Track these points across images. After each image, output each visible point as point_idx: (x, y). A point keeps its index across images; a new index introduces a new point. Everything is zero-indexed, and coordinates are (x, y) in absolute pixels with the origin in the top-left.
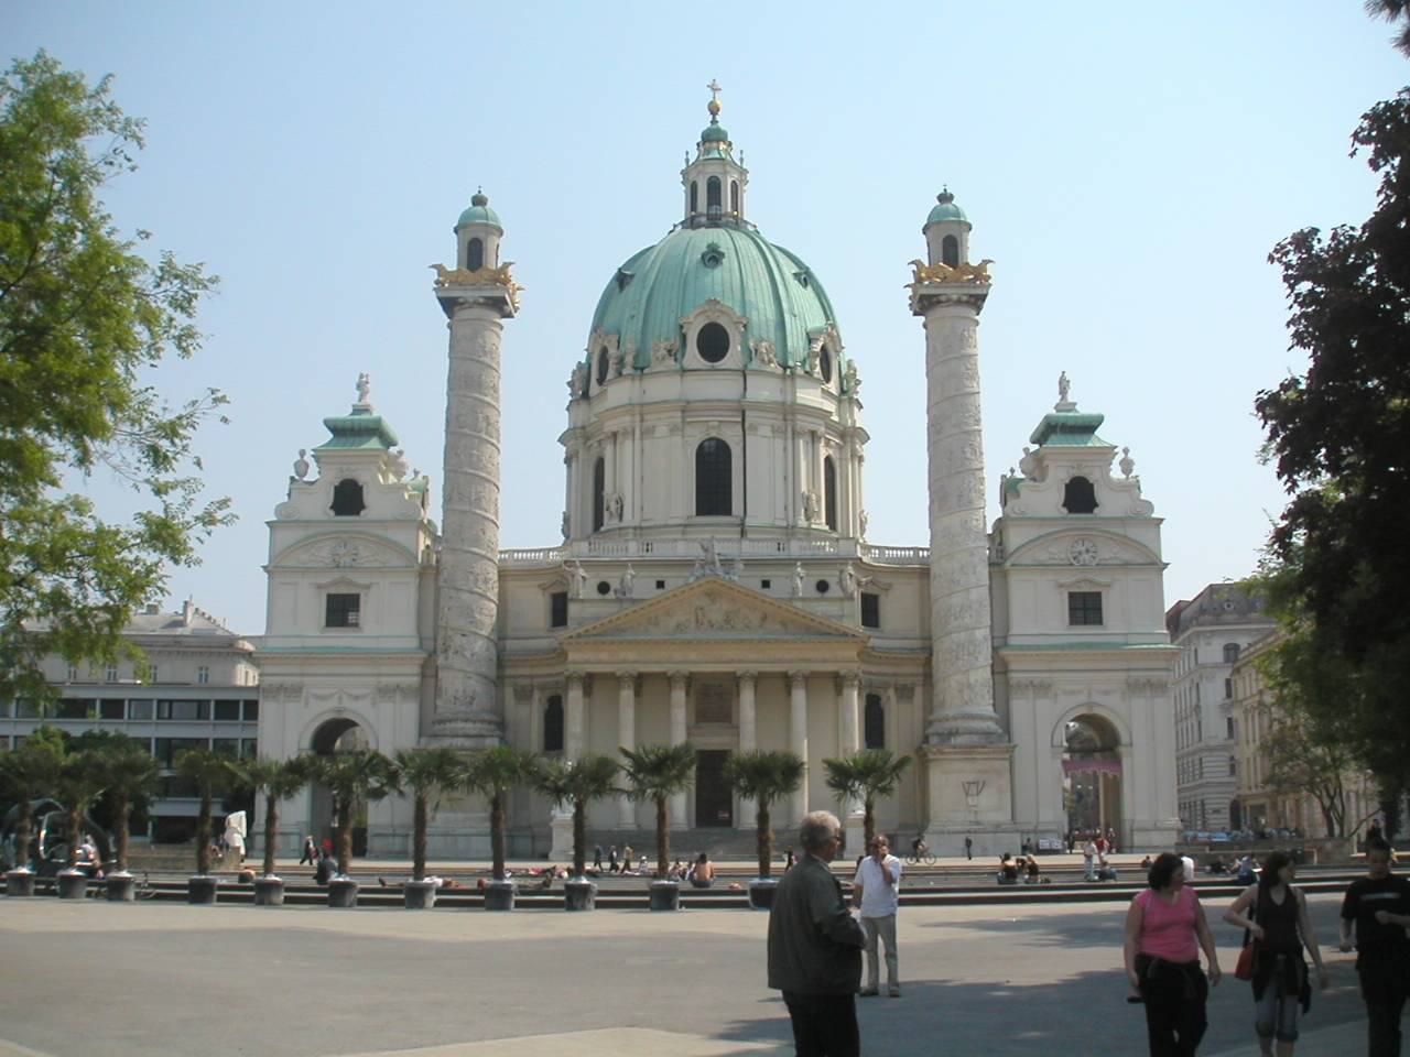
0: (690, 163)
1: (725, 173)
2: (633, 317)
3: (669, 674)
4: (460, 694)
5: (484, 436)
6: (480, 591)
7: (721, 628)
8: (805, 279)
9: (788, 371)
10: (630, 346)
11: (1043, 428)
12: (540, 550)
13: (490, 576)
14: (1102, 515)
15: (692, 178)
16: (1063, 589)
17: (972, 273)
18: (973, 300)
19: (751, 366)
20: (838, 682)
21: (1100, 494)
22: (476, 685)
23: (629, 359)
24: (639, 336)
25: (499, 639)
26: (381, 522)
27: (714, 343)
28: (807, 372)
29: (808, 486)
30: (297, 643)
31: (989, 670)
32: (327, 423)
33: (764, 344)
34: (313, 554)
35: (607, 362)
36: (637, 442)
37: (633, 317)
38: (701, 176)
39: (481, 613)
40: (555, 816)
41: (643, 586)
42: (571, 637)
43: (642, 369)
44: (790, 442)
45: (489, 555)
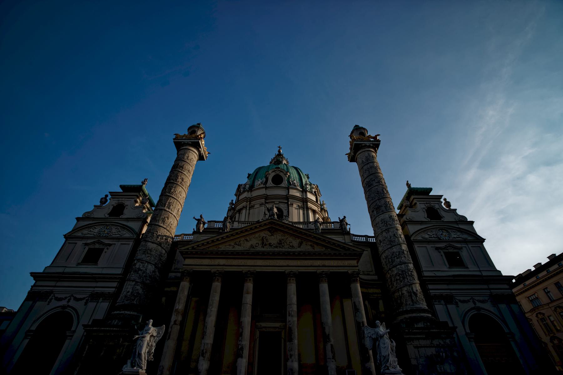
4: (129, 294)
5: (179, 184)
7: (276, 247)
11: (407, 195)
14: (445, 221)
17: (372, 138)
18: (374, 146)
19: (290, 186)
21: (443, 213)
26: (128, 219)
27: (278, 180)
30: (60, 270)
32: (121, 186)
34: (91, 231)
42: (188, 249)
44: (305, 212)
45: (168, 229)
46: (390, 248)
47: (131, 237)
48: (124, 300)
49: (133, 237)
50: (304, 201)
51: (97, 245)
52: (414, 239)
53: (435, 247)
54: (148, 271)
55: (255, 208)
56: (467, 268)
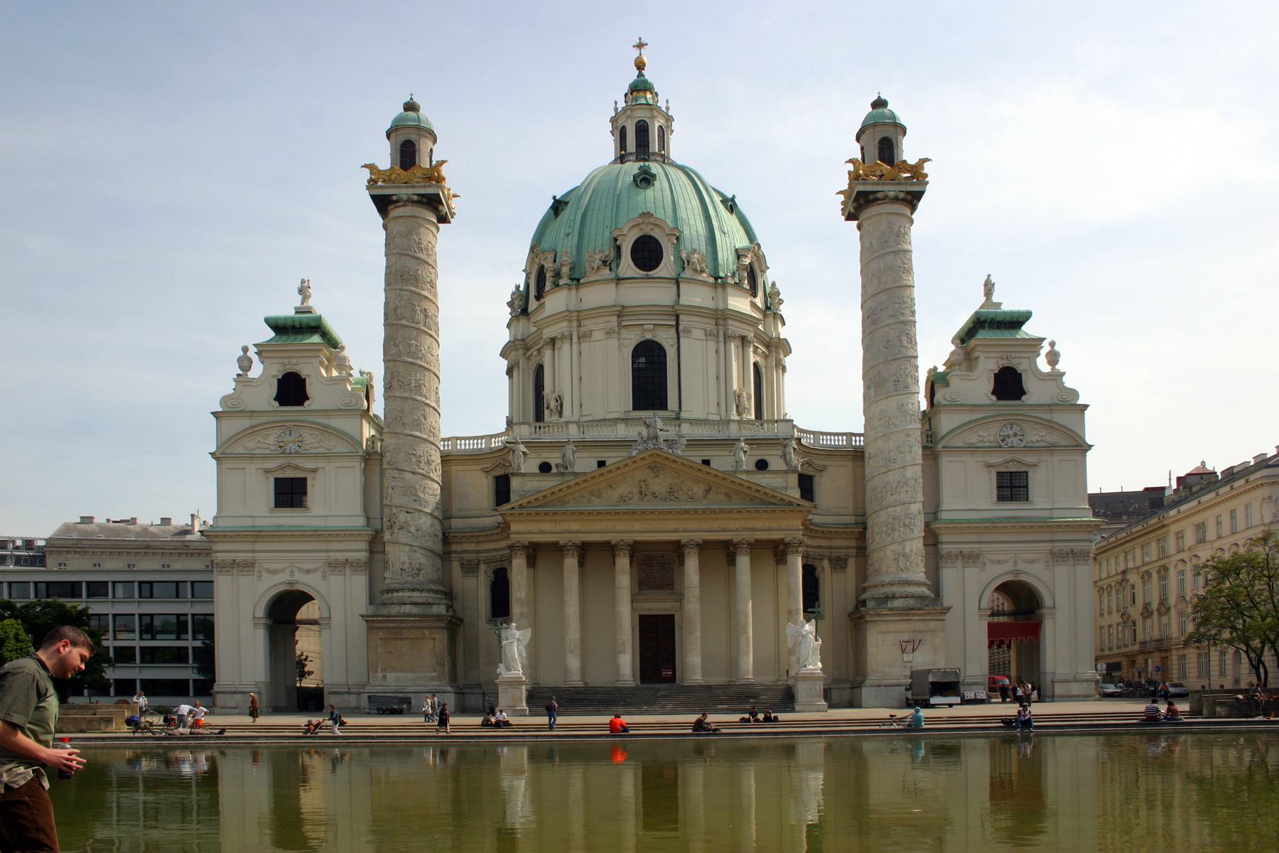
0: (620, 109)
1: (653, 117)
2: (568, 235)
3: (613, 542)
4: (406, 566)
6: (424, 472)
8: (731, 205)
9: (720, 281)
10: (566, 258)
12: (482, 437)
13: (433, 458)
15: (620, 124)
16: (991, 469)
19: (683, 275)
20: (778, 551)
22: (422, 559)
23: (565, 270)
24: (574, 252)
25: (443, 519)
28: (737, 283)
29: (739, 386)
30: (247, 523)
31: (921, 540)
33: (696, 255)
35: (545, 277)
36: (575, 346)
37: (568, 235)
38: (629, 121)
39: (424, 492)
40: (500, 674)
41: (585, 463)
43: (578, 280)
44: (722, 344)
46: (883, 473)
47: (352, 452)
48: (401, 575)
49: (356, 453)
50: (719, 316)
51: (290, 472)
52: (947, 445)
53: (983, 462)
54: (424, 528)
55: (595, 341)
56: (1032, 502)
